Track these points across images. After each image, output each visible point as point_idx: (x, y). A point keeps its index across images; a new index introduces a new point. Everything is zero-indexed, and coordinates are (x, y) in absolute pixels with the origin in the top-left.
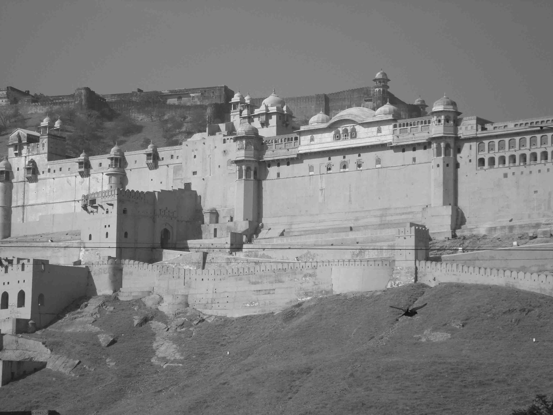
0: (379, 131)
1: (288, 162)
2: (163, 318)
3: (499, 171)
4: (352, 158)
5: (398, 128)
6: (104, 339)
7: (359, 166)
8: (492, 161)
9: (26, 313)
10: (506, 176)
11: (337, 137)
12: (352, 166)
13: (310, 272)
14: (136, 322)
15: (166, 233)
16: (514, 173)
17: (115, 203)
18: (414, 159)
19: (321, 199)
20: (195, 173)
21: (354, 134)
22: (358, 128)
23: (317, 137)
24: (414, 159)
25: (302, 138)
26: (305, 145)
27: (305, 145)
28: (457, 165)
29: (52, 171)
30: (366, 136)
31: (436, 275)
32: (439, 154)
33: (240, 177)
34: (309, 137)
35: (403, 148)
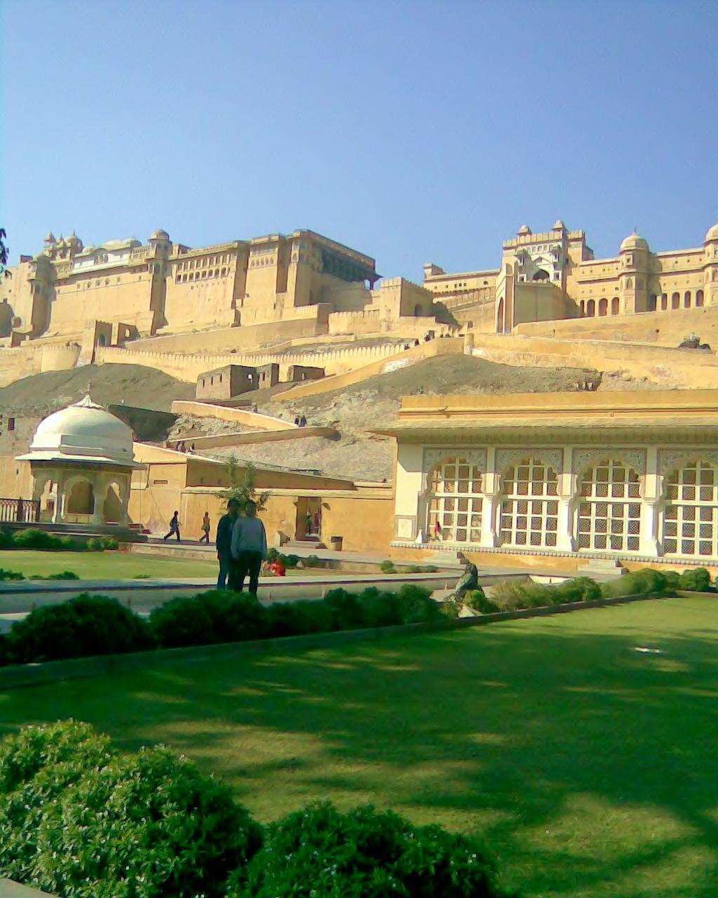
3: (189, 284)
5: (132, 255)
7: (107, 283)
10: (192, 288)
11: (96, 262)
12: (103, 283)
13: (30, 356)
16: (197, 286)
18: (140, 277)
21: (106, 260)
22: (109, 255)
24: (140, 277)
27: (79, 268)
30: (114, 261)
31: (108, 356)
32: (150, 273)
33: (32, 292)
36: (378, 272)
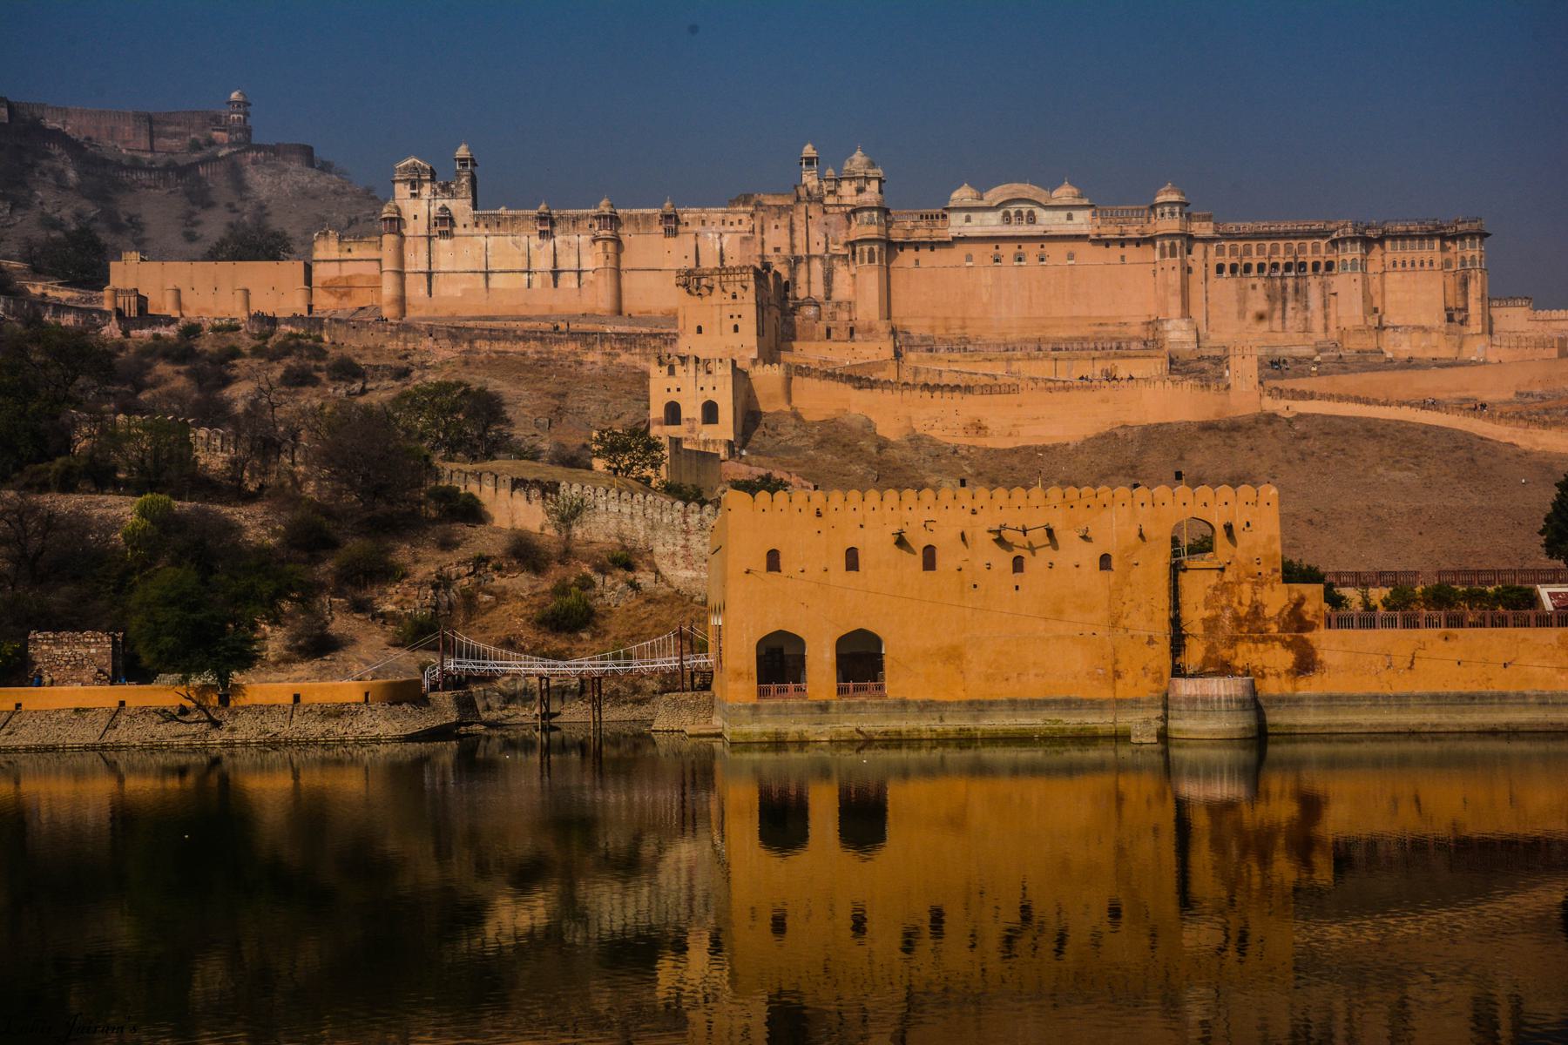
0: (1070, 217)
1: (933, 245)
4: (1031, 250)
8: (1248, 268)
10: (1254, 287)
17: (752, 286)
18: (1123, 258)
19: (985, 298)
20: (777, 250)
21: (1032, 219)
22: (1038, 211)
24: (1123, 258)
25: (952, 217)
26: (956, 225)
27: (956, 225)
29: (482, 225)
30: (1050, 221)
33: (871, 260)
34: (964, 215)
35: (1108, 243)
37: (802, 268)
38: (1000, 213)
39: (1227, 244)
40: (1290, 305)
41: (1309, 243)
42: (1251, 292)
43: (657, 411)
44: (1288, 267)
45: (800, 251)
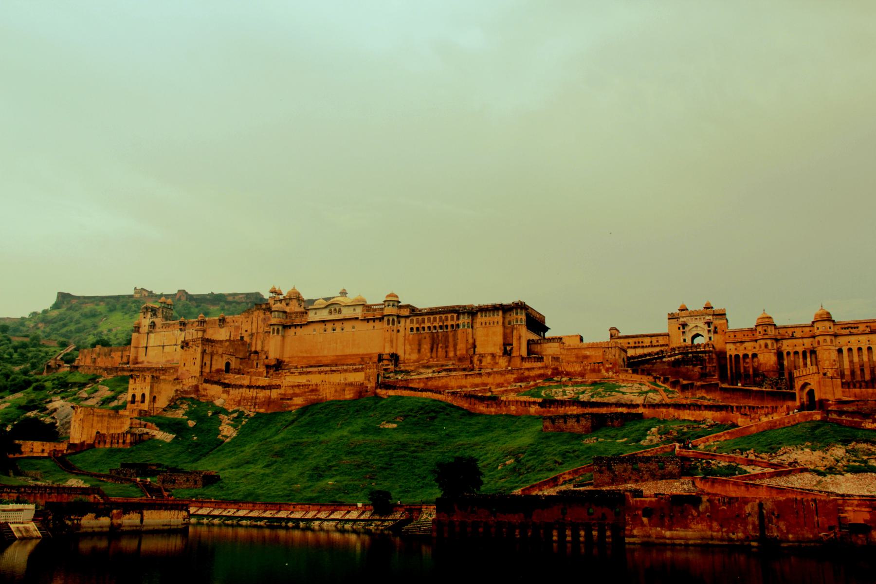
1: (301, 326)
2: (226, 412)
4: (338, 326)
6: (191, 423)
9: (145, 406)
14: (210, 414)
15: (228, 364)
21: (340, 311)
23: (318, 312)
27: (312, 316)
28: (398, 331)
30: (347, 313)
32: (388, 324)
34: (314, 311)
35: (368, 320)
36: (547, 324)
37: (254, 338)
38: (327, 310)
39: (415, 318)
40: (440, 345)
41: (449, 316)
42: (424, 341)
43: (130, 399)
44: (441, 327)
45: (254, 331)
